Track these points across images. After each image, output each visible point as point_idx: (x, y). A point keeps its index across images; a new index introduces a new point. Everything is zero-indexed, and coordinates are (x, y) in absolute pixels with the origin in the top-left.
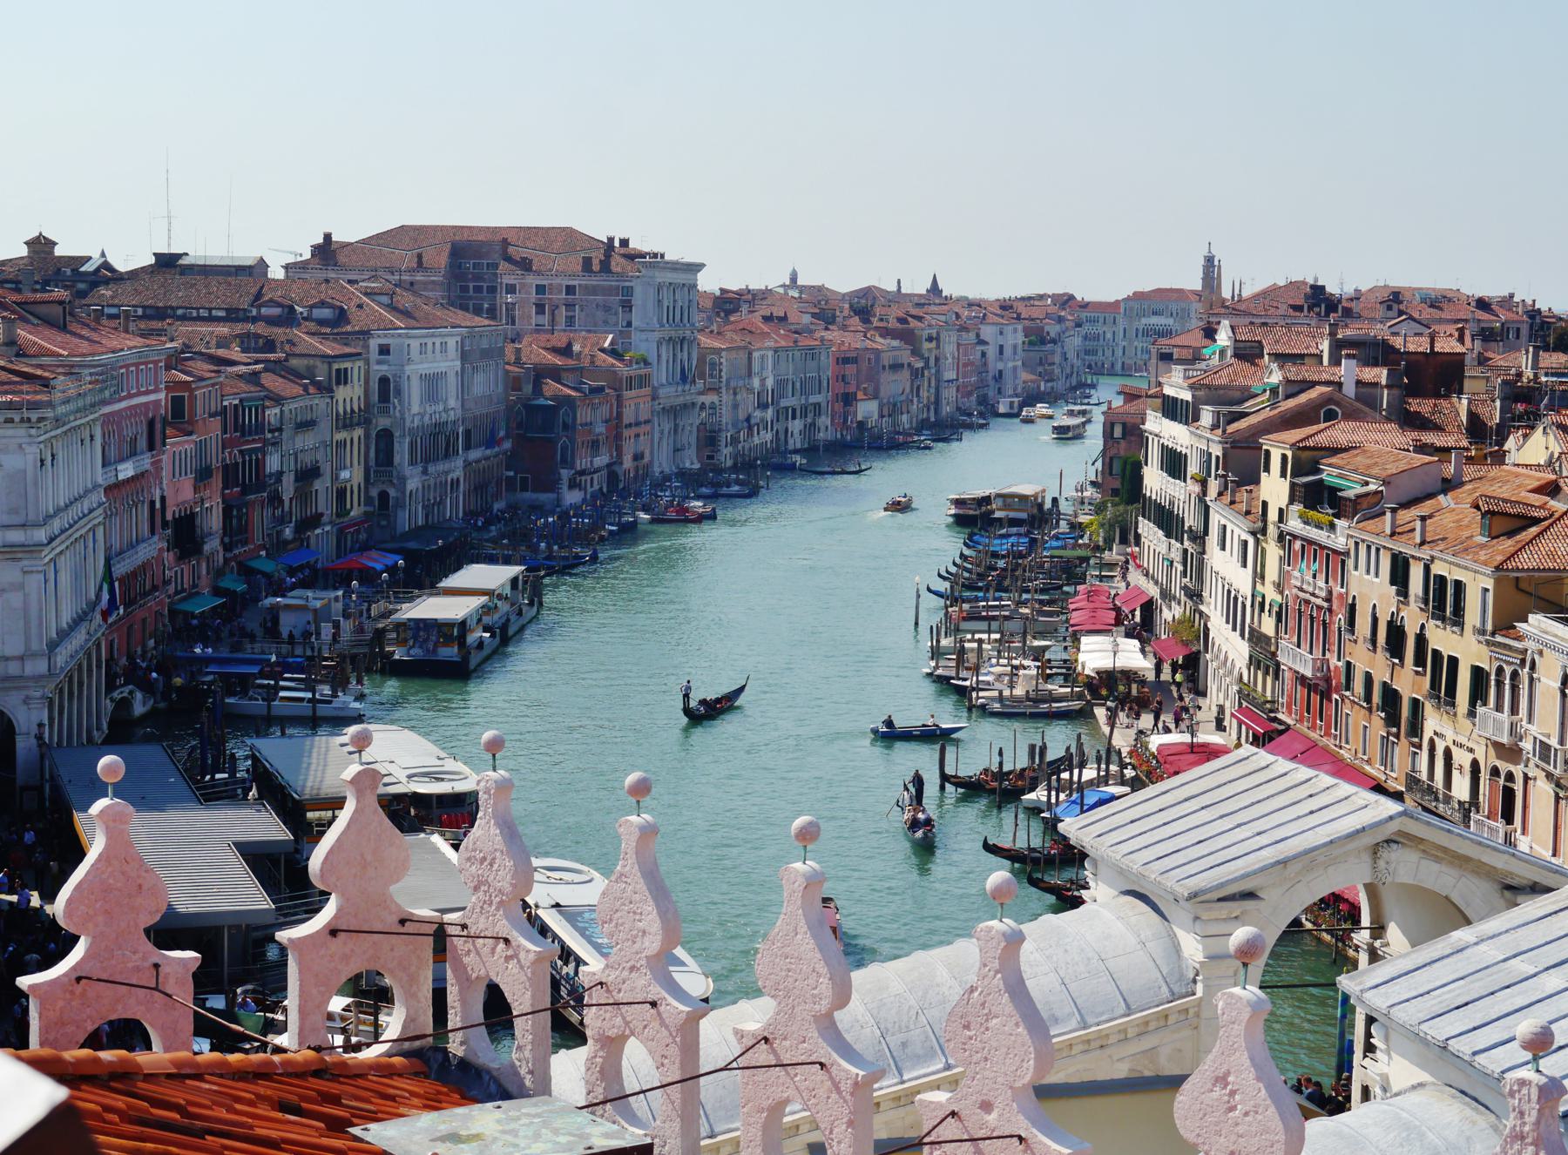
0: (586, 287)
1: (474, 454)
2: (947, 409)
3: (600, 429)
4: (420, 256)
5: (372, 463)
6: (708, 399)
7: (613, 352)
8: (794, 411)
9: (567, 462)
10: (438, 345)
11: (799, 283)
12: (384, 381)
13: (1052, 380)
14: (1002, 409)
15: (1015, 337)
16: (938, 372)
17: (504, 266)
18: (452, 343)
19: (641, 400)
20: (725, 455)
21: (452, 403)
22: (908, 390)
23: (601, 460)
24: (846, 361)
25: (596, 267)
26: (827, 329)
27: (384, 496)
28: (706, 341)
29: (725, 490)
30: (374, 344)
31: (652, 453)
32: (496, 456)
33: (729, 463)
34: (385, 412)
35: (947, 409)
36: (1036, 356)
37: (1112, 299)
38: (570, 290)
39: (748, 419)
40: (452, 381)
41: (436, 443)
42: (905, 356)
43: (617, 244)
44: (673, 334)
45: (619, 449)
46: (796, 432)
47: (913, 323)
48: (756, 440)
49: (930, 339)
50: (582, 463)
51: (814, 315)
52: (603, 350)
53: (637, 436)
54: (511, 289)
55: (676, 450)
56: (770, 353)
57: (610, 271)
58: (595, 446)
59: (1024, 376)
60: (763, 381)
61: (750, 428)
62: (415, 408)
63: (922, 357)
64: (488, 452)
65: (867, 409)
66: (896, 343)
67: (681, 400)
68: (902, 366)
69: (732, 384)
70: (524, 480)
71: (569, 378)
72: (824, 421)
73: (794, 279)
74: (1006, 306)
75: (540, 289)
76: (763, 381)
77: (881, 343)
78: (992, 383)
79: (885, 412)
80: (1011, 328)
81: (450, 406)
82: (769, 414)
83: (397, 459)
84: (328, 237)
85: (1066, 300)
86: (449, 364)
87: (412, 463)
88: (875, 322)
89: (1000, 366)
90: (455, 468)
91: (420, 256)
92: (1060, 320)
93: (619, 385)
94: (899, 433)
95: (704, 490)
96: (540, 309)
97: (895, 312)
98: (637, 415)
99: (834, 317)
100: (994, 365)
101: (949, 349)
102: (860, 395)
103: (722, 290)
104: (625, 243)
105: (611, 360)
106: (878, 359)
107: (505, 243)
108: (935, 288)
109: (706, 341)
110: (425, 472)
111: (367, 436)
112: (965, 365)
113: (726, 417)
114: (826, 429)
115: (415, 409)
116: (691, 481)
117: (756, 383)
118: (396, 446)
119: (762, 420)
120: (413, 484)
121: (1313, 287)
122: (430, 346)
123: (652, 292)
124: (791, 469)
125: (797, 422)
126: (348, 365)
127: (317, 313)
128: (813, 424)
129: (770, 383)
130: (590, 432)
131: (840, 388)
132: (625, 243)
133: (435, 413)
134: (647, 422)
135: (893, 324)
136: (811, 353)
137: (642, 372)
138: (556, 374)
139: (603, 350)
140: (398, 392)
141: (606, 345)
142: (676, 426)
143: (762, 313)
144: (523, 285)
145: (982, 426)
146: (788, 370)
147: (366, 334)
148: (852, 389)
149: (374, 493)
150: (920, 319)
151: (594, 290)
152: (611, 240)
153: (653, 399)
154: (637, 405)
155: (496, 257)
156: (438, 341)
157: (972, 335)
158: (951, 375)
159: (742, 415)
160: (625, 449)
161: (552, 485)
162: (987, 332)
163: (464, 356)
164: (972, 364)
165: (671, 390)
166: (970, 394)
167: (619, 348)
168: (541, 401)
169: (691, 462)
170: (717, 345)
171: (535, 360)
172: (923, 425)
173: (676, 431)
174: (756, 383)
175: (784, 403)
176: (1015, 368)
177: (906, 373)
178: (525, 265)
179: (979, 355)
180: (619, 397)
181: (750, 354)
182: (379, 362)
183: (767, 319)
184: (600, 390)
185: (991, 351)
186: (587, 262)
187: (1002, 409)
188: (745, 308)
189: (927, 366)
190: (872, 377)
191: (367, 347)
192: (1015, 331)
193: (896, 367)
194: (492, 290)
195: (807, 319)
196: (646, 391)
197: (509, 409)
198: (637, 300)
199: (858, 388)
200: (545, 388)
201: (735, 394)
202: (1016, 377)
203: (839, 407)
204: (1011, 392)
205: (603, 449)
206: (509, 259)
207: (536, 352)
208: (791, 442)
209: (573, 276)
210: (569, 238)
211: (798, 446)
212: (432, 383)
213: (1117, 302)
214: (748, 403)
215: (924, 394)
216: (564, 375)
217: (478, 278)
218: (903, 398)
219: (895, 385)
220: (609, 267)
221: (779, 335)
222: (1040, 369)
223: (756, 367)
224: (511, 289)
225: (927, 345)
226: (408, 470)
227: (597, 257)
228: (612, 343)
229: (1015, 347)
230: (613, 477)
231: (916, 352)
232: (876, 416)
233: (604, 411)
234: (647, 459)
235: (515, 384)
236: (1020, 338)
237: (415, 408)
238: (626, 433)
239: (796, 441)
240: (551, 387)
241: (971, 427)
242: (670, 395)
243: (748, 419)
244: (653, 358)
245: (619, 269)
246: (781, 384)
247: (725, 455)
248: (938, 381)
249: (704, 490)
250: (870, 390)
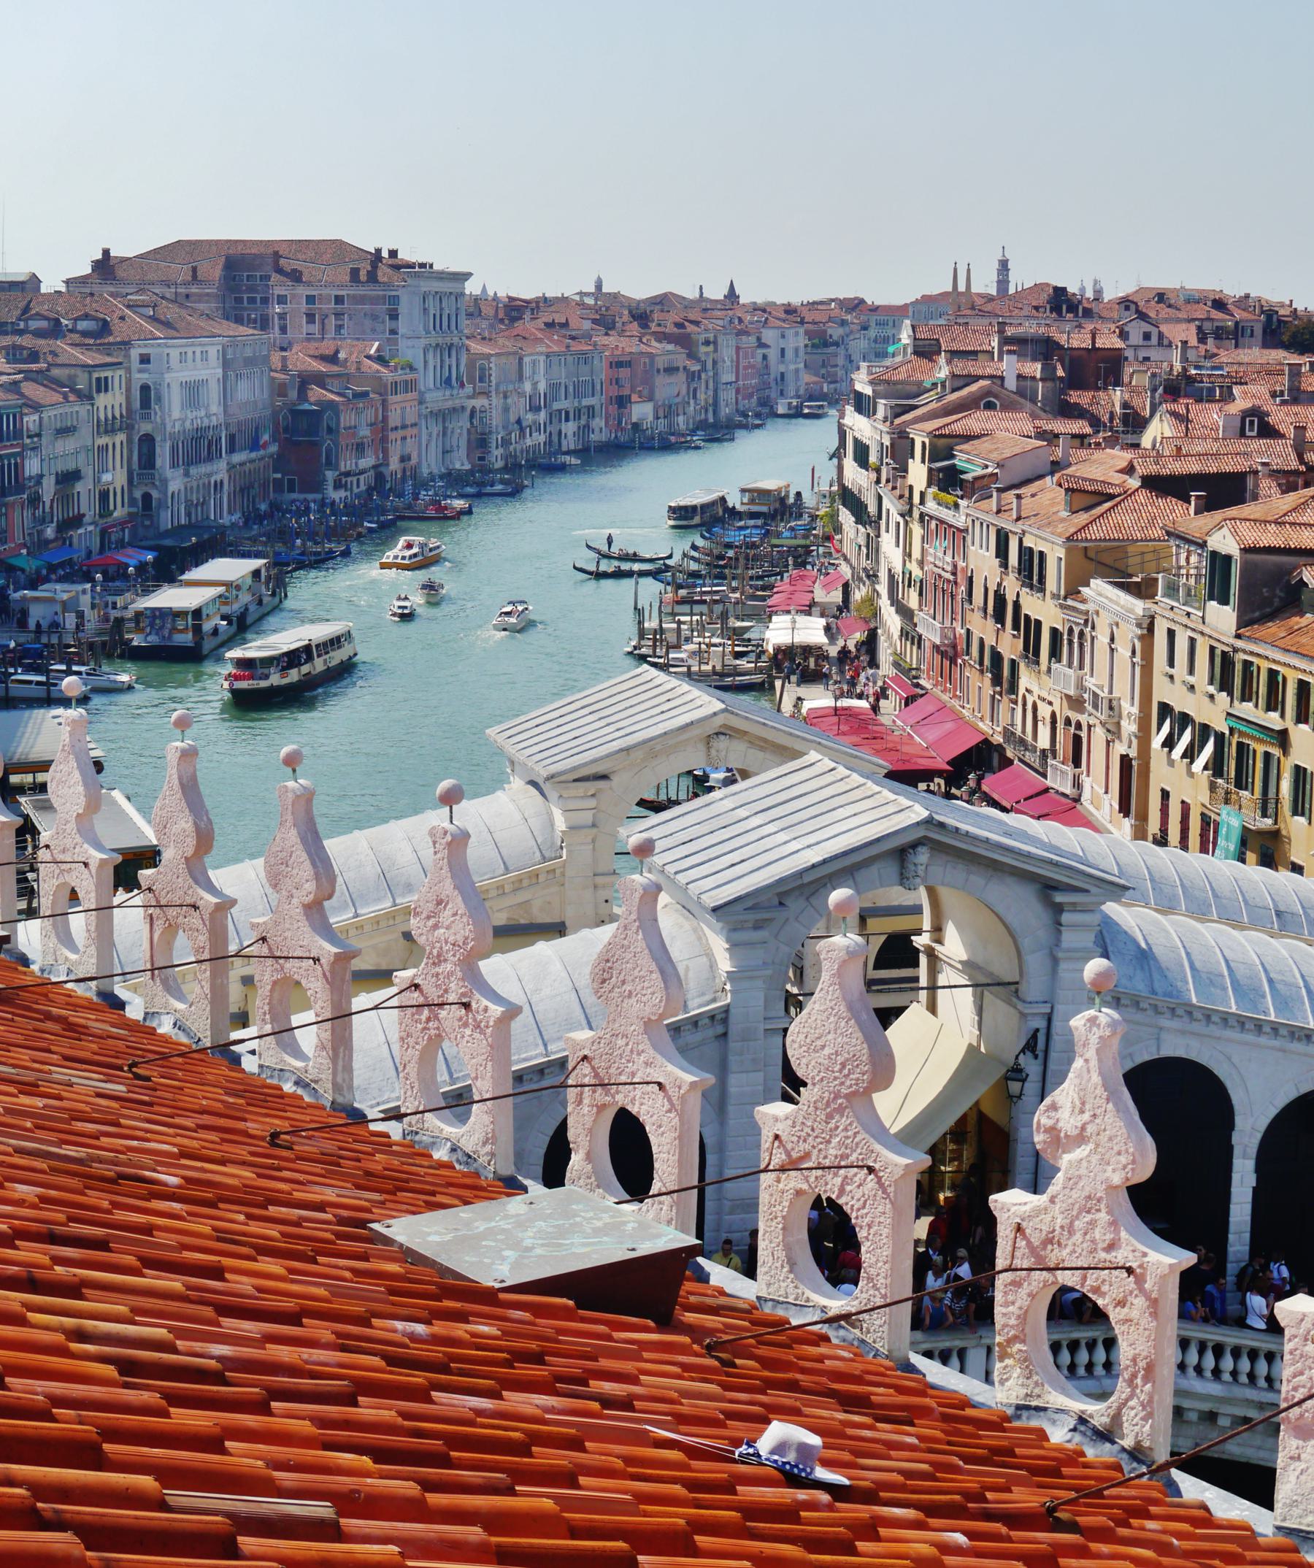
0: (354, 297)
1: (238, 458)
2: (725, 411)
3: (365, 432)
4: (194, 270)
5: (135, 466)
6: (479, 403)
7: (380, 359)
8: (567, 413)
9: (330, 464)
10: (198, 354)
11: (604, 290)
12: (145, 389)
13: (836, 382)
14: (781, 410)
15: (797, 340)
16: (716, 374)
17: (275, 277)
18: (213, 352)
19: (408, 404)
20: (496, 457)
21: (215, 408)
22: (684, 391)
23: (367, 462)
24: (620, 364)
26: (607, 334)
27: (147, 497)
28: (476, 347)
29: (488, 489)
30: (135, 353)
31: (419, 455)
32: (262, 458)
33: (500, 464)
34: (146, 417)
35: (725, 411)
36: (819, 359)
37: (900, 302)
38: (339, 300)
39: (519, 422)
41: (199, 447)
42: (681, 359)
43: (385, 254)
44: (440, 341)
45: (385, 451)
46: (570, 434)
47: (690, 328)
48: (529, 442)
49: (707, 343)
50: (346, 464)
51: (594, 321)
52: (369, 357)
53: (404, 438)
54: (282, 300)
55: (445, 452)
56: (542, 358)
57: (377, 281)
58: (360, 448)
59: (807, 378)
60: (535, 384)
61: (522, 430)
62: (175, 415)
63: (698, 360)
64: (253, 455)
65: (641, 411)
66: (670, 347)
67: (449, 404)
68: (677, 369)
69: (502, 388)
70: (291, 482)
71: (335, 384)
72: (598, 423)
73: (599, 285)
74: (790, 310)
75: (311, 299)
76: (535, 384)
77: (657, 347)
78: (773, 384)
79: (661, 414)
80: (792, 331)
81: (212, 411)
82: (542, 416)
83: (158, 463)
84: (106, 252)
85: (856, 305)
86: (210, 371)
87: (174, 465)
88: (653, 327)
89: (782, 368)
90: (219, 470)
91: (194, 270)
92: (843, 323)
93: (385, 391)
94: (673, 434)
95: (469, 490)
96: (311, 318)
97: (674, 317)
98: (403, 418)
99: (614, 322)
100: (776, 368)
101: (727, 353)
102: (634, 398)
103: (509, 298)
104: (393, 253)
105: (376, 366)
106: (652, 363)
107: (277, 255)
108: (732, 295)
109: (476, 347)
110: (187, 474)
111: (130, 440)
112: (745, 368)
113: (496, 420)
114: (600, 431)
115: (176, 414)
116: (454, 480)
117: (527, 387)
118: (158, 450)
119: (534, 422)
120: (176, 483)
121: (1056, 289)
122: (190, 354)
123: (417, 300)
124: (562, 468)
125: (571, 424)
126: (109, 374)
127: (82, 325)
128: (587, 426)
129: (542, 387)
130: (354, 434)
131: (614, 391)
132: (393, 253)
133: (196, 418)
134: (415, 425)
135: (670, 329)
136: (584, 358)
137: (408, 377)
138: (320, 380)
139: (369, 357)
140: (159, 399)
141: (372, 352)
142: (445, 428)
143: (545, 320)
144: (293, 296)
145: (758, 426)
146: (561, 375)
147: (126, 344)
148: (626, 392)
149: (138, 494)
150: (697, 323)
151: (361, 300)
152: (378, 251)
153: (420, 403)
154: (403, 409)
155: (268, 269)
156: (198, 350)
157: (752, 339)
158: (728, 377)
159: (513, 418)
160: (391, 448)
161: (317, 486)
162: (769, 336)
163: (226, 364)
164: (752, 367)
165: (438, 395)
166: (751, 395)
167: (387, 355)
168: (306, 406)
169: (461, 463)
170: (486, 350)
171: (300, 367)
172: (701, 425)
173: (444, 434)
174: (527, 387)
175: (556, 406)
176: (797, 371)
177: (682, 376)
178: (296, 276)
179: (759, 358)
180: (384, 402)
181: (521, 359)
182: (140, 371)
183: (550, 325)
184: (365, 394)
185: (773, 354)
186: (355, 273)
187: (781, 410)
188: (527, 316)
189: (704, 369)
190: (648, 380)
191: (128, 356)
192: (797, 334)
193: (671, 370)
194: (265, 301)
195: (587, 325)
196: (414, 395)
197: (275, 414)
198: (403, 309)
199: (633, 390)
200: (310, 394)
201: (505, 397)
202: (797, 379)
203: (613, 409)
204: (792, 394)
205: (369, 452)
206: (280, 271)
207: (302, 360)
208: (564, 443)
209: (341, 286)
210: (339, 246)
211: (572, 447)
212: (193, 391)
213: (906, 305)
214: (519, 407)
215: (701, 396)
216: (328, 380)
217: (252, 289)
218: (677, 400)
219: (670, 388)
220: (375, 279)
221: (552, 341)
222: (823, 371)
223: (527, 371)
224: (282, 300)
225: (703, 349)
226: (169, 473)
227: (365, 268)
228: (378, 350)
229: (797, 350)
230: (380, 477)
231: (692, 356)
232: (651, 418)
233: (369, 415)
234: (414, 461)
235: (281, 390)
236: (802, 341)
237: (175, 415)
238: (392, 436)
239: (570, 443)
240: (316, 393)
241: (745, 427)
242: (438, 399)
243: (519, 422)
244: (419, 365)
245: (385, 279)
246: (554, 387)
247: (496, 457)
248: (716, 383)
249: (469, 490)
250: (646, 393)
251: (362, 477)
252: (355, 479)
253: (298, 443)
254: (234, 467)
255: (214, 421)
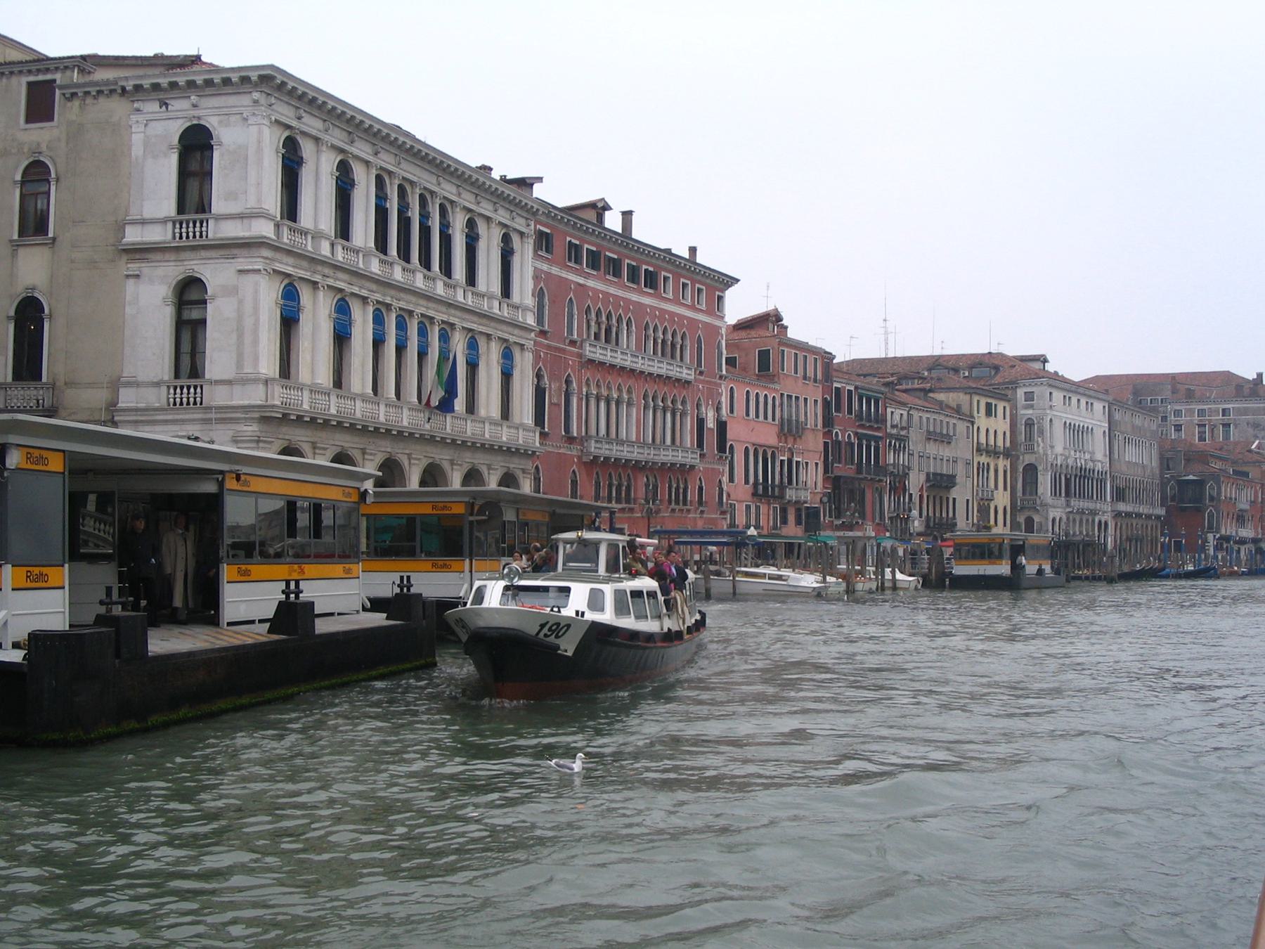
1: (1122, 507)
5: (1020, 494)
18: (1098, 406)
21: (1099, 456)
25: (1246, 391)
27: (1029, 521)
30: (1020, 393)
32: (1149, 517)
40: (1098, 433)
50: (1228, 529)
58: (1241, 519)
62: (1055, 448)
83: (1040, 491)
110: (1068, 505)
115: (1059, 449)
122: (1074, 400)
140: (1041, 432)
147: (1014, 384)
149: (1021, 519)
151: (1245, 412)
155: (1167, 394)
168: (1191, 477)
182: (1027, 407)
210: (1227, 377)
212: (1077, 433)
226: (1048, 498)
237: (1055, 448)
251: (1243, 548)
252: (1236, 547)
253: (1184, 510)
254: (1118, 515)
255: (1099, 467)
